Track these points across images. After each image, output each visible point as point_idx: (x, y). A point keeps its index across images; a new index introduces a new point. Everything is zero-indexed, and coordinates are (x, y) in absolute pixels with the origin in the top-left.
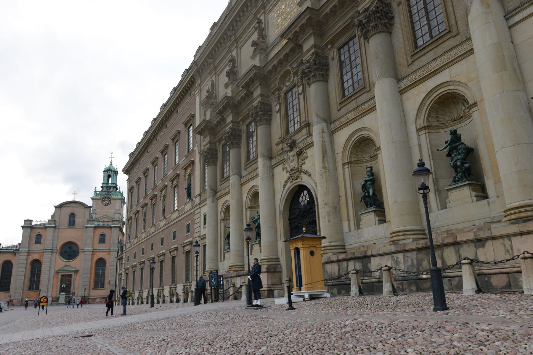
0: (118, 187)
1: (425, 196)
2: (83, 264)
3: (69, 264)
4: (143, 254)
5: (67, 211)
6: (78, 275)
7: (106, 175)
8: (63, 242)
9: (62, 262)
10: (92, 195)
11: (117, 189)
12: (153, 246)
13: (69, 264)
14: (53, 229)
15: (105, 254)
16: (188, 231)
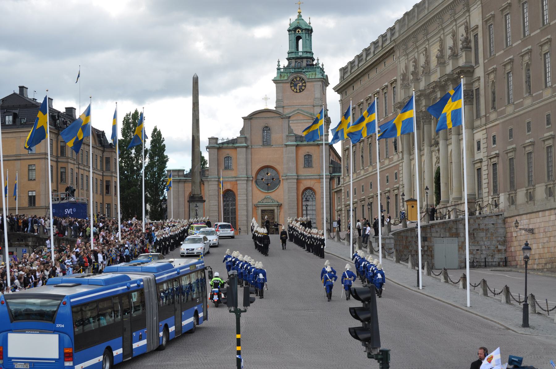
0: (315, 57)
2: (284, 194)
3: (269, 195)
5: (259, 124)
6: (282, 210)
7: (294, 37)
8: (258, 167)
9: (260, 193)
11: (313, 60)
12: (371, 185)
13: (269, 195)
14: (245, 149)
16: (396, 178)
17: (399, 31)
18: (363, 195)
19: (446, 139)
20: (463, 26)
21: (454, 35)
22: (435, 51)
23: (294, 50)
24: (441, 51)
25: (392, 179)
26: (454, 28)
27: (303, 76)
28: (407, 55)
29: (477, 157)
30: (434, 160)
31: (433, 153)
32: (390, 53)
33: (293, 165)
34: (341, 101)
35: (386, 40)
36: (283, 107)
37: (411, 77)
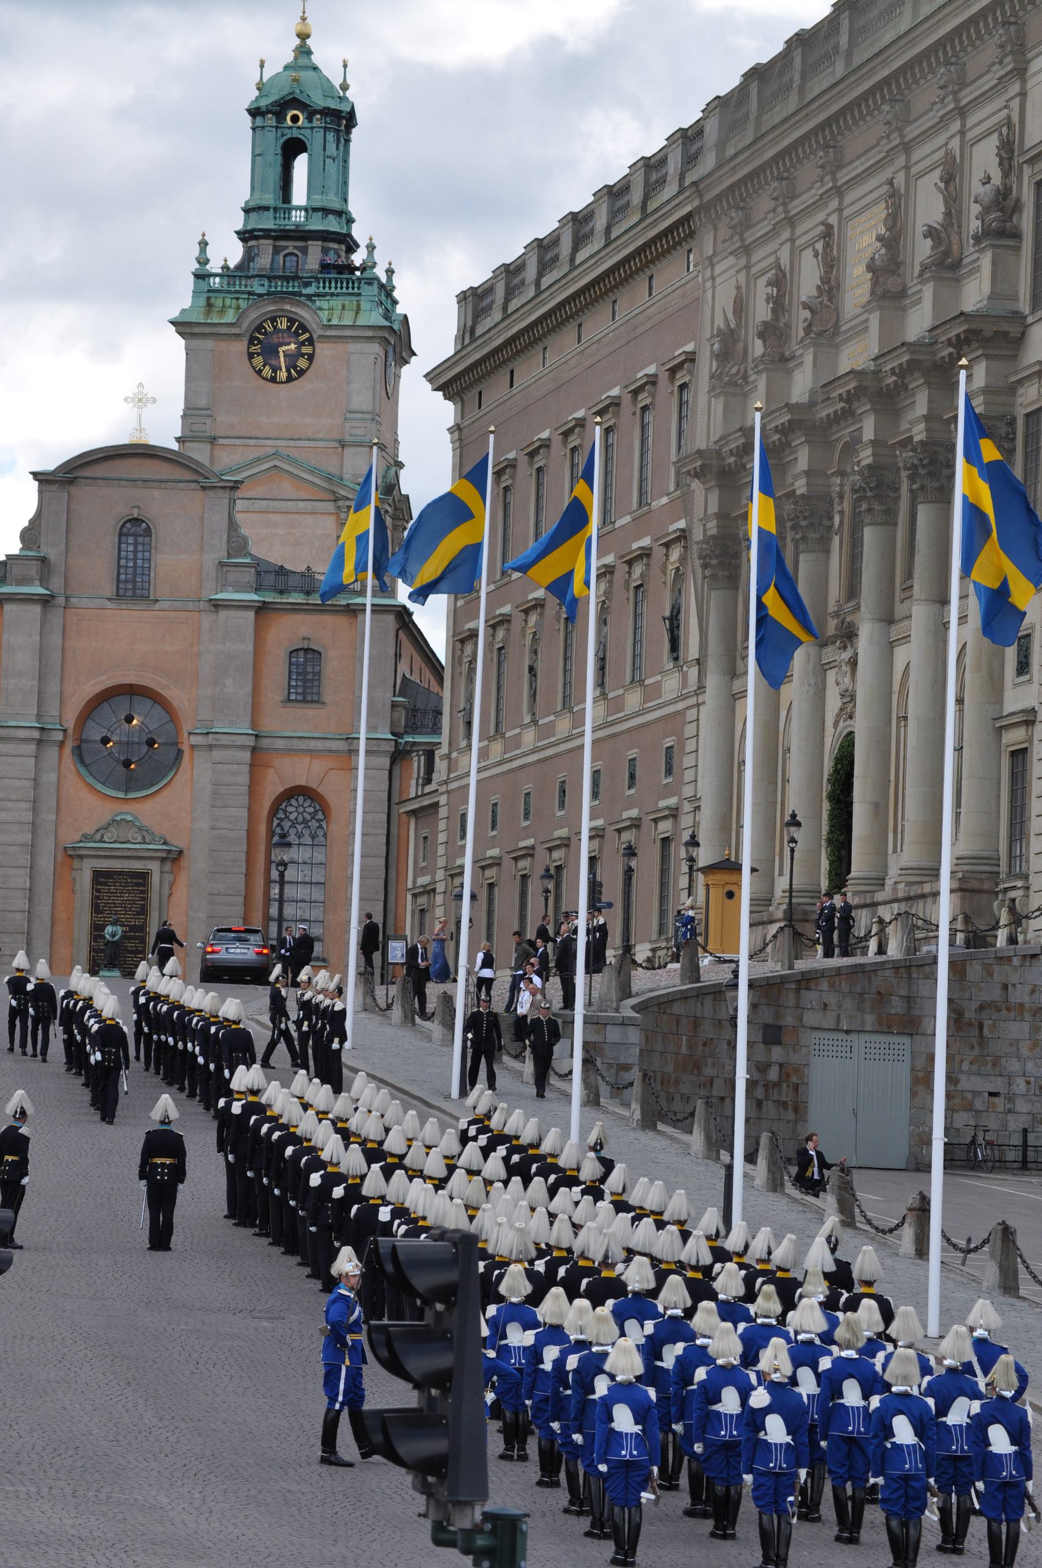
0: (358, 232)
1: (546, 899)
2: (196, 809)
3: (128, 811)
4: (526, 816)
6: (183, 879)
7: (273, 144)
8: (90, 689)
9: (90, 799)
10: (182, 298)
12: (563, 792)
13: (128, 811)
14: (37, 609)
15: (318, 766)
16: (669, 771)
17: (721, 146)
18: (527, 833)
19: (888, 618)
20: (994, 141)
21: (952, 176)
22: (863, 240)
23: (270, 199)
24: (893, 240)
25: (652, 772)
26: (955, 144)
27: (303, 314)
28: (746, 250)
29: (1015, 700)
30: (833, 703)
31: (831, 676)
32: (677, 236)
33: (237, 689)
34: (456, 429)
35: (662, 181)
36: (213, 440)
37: (758, 348)
